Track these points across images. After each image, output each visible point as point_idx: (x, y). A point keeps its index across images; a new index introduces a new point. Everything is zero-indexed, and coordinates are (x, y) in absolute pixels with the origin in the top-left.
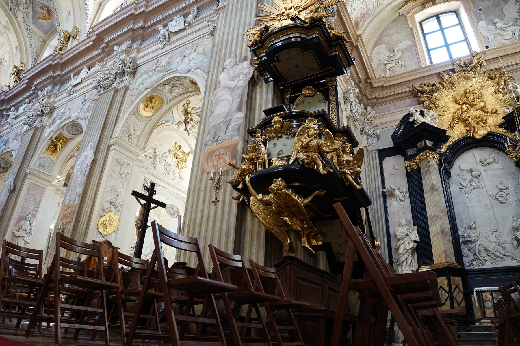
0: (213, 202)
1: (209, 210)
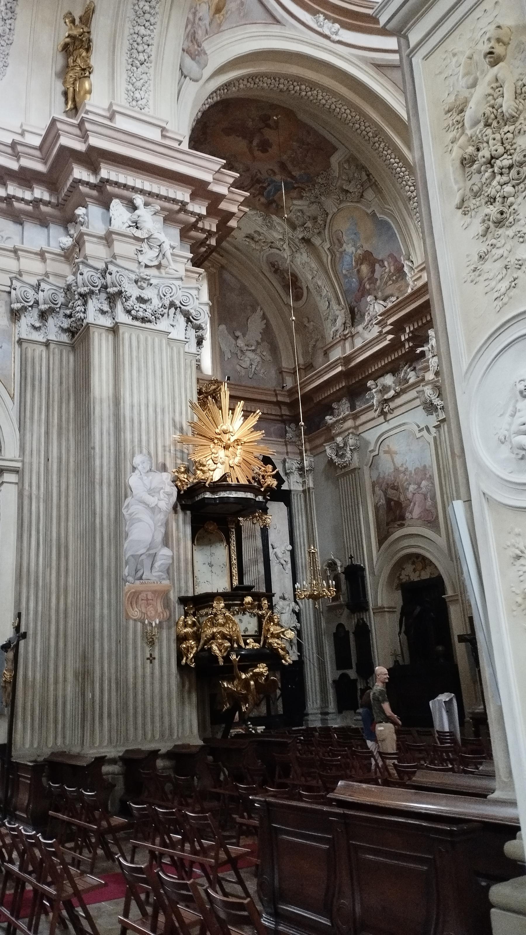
0: (148, 659)
1: (144, 668)
